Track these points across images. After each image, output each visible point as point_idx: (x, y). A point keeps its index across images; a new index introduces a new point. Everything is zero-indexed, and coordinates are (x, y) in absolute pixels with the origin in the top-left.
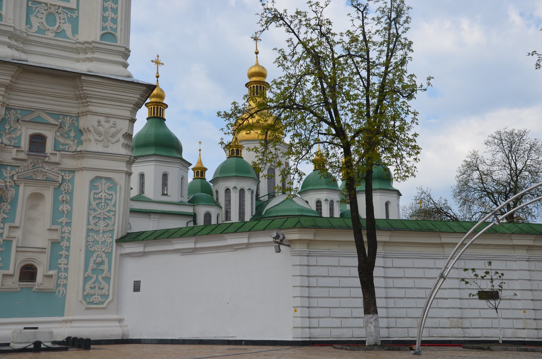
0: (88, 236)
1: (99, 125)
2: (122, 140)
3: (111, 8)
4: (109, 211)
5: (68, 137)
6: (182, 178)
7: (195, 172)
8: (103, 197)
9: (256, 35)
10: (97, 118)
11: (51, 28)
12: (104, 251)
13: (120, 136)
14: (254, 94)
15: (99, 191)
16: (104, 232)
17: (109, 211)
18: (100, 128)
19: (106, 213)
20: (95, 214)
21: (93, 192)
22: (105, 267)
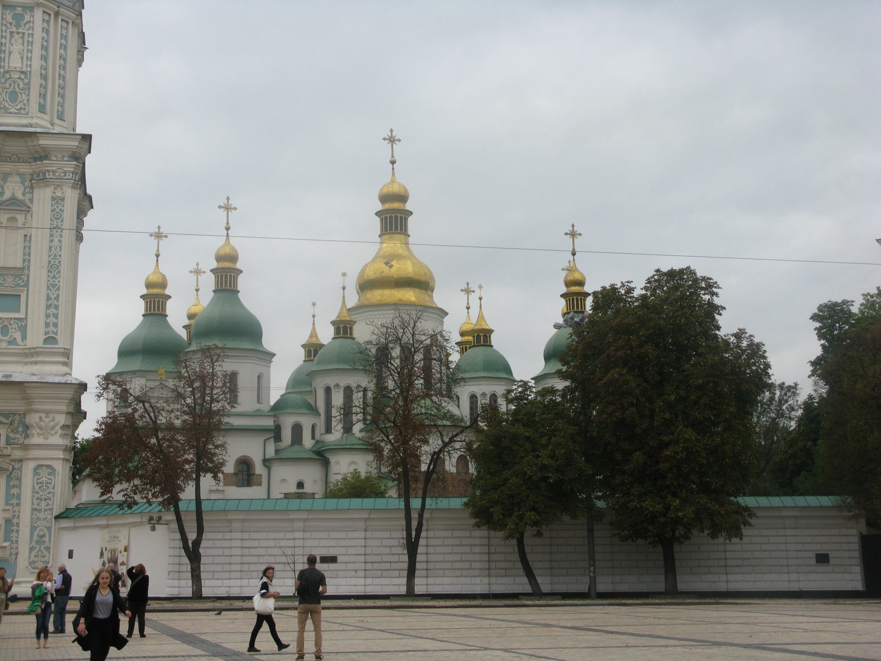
0: (32, 514)
1: (40, 421)
2: (60, 432)
3: (53, 314)
4: (49, 493)
5: (17, 432)
6: (259, 377)
7: (305, 351)
8: (44, 481)
9: (392, 133)
10: (38, 415)
11: (4, 338)
12: (45, 526)
13: (58, 428)
14: (386, 230)
15: (41, 476)
16: (45, 510)
17: (49, 493)
18: (42, 423)
19: (47, 495)
20: (38, 496)
21: (36, 477)
22: (46, 539)
